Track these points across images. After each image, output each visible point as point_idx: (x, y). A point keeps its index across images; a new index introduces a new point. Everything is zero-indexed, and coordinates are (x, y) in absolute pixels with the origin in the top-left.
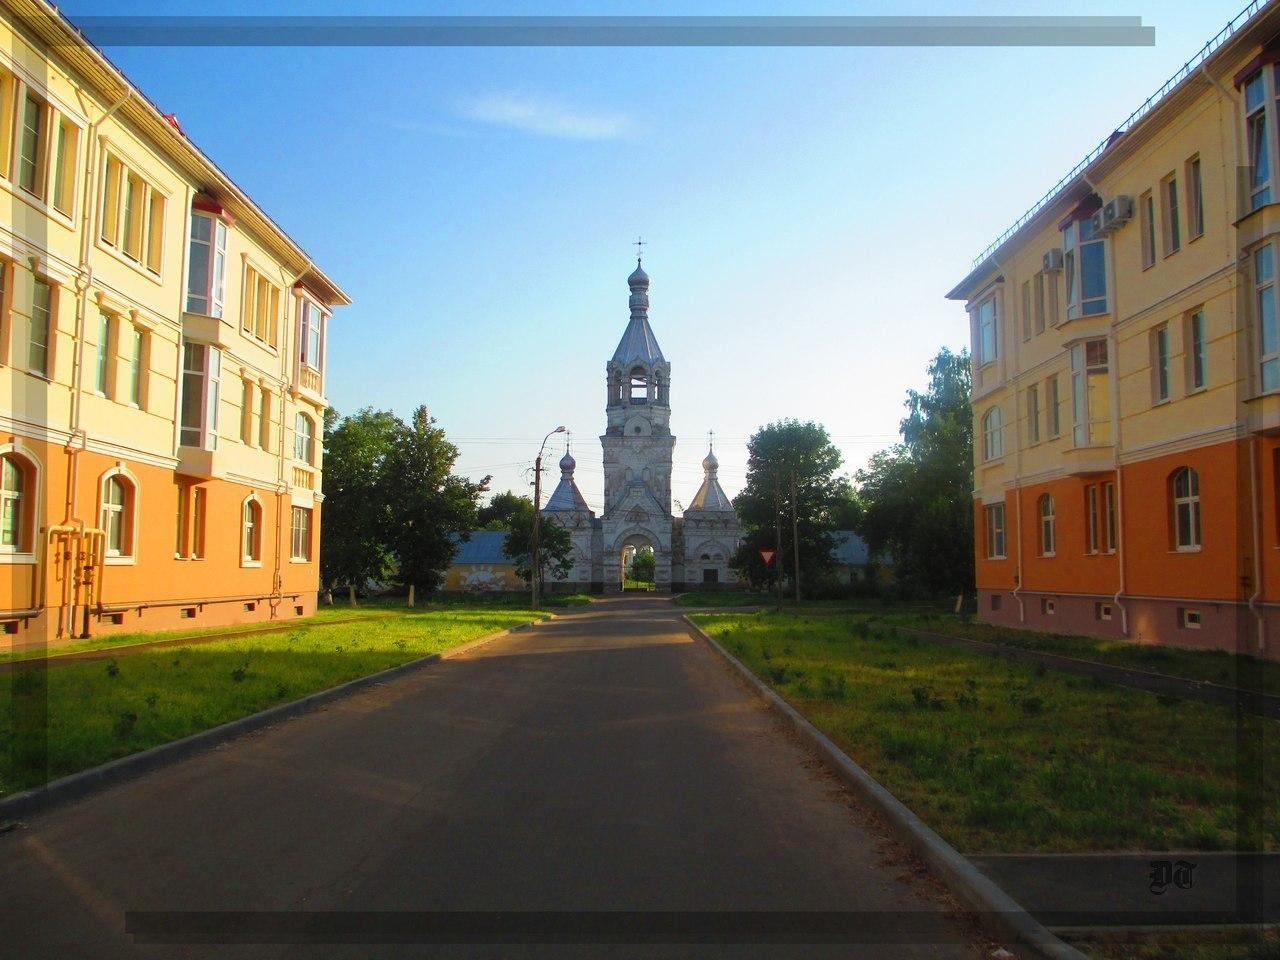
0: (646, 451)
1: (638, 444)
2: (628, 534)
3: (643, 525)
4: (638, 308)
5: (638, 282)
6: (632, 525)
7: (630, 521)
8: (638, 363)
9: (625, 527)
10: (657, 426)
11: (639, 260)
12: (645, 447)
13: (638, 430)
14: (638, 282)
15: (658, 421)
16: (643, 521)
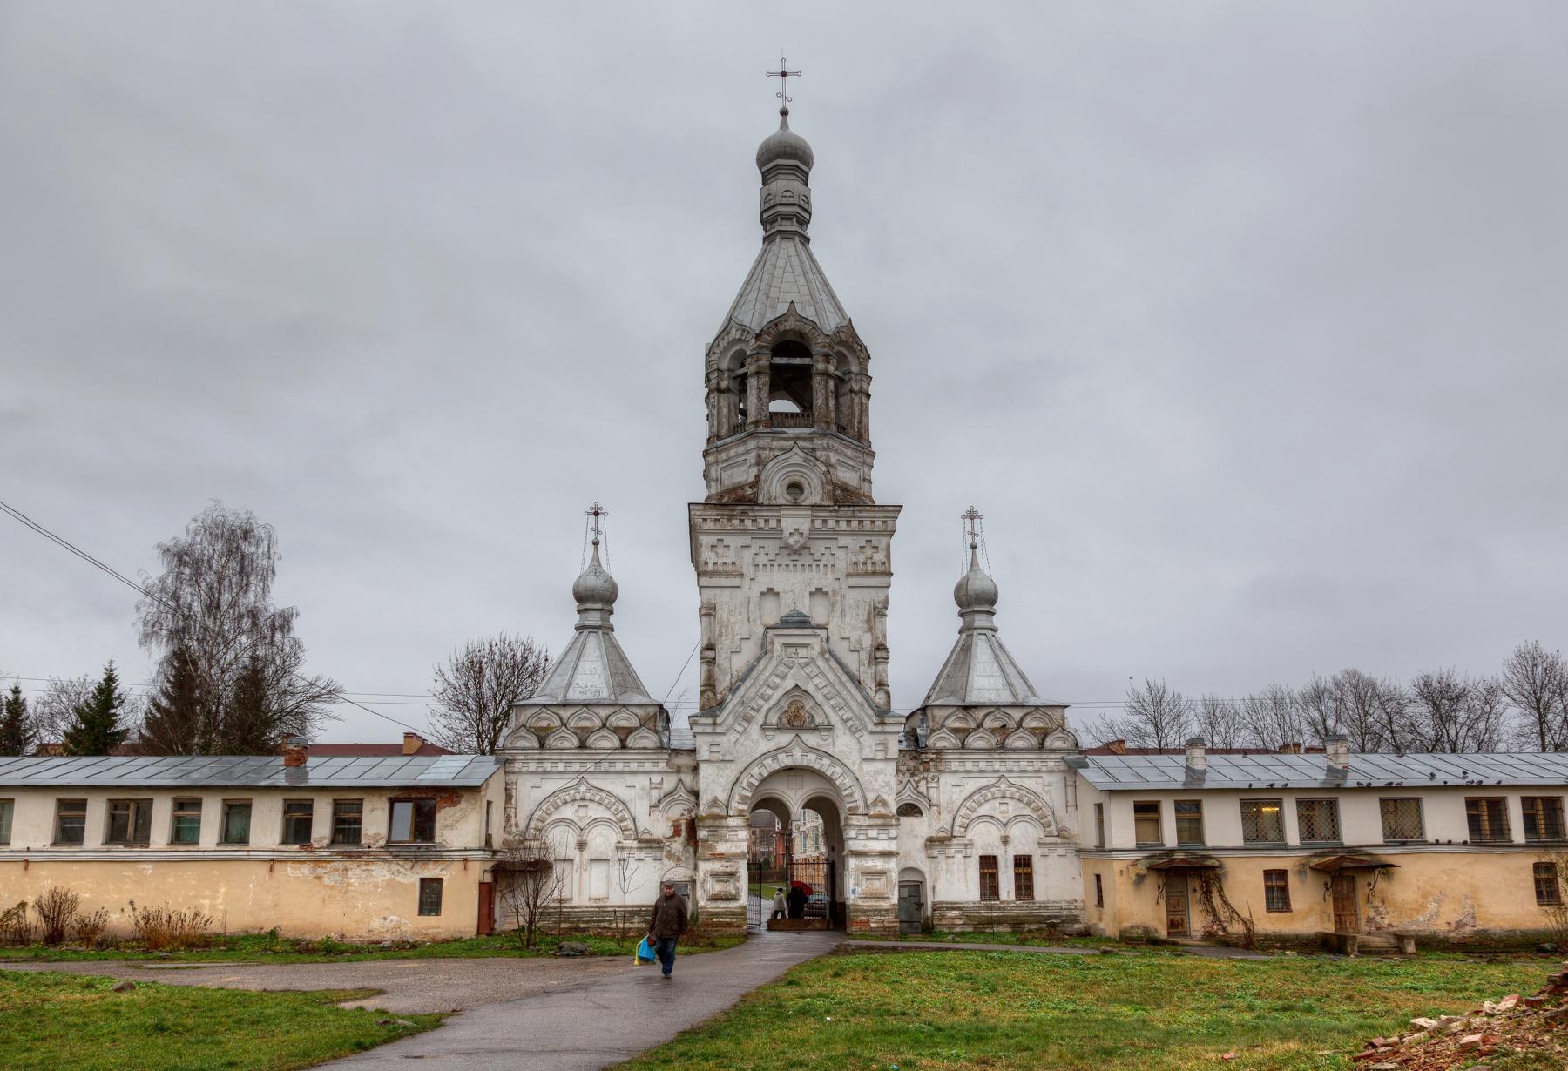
0: (818, 547)
1: (794, 524)
2: (772, 765)
3: (812, 739)
4: (785, 221)
5: (784, 161)
6: (784, 738)
7: (779, 728)
8: (789, 325)
9: (772, 745)
10: (844, 488)
11: (784, 113)
12: (814, 534)
13: (795, 487)
14: (784, 161)
15: (847, 476)
16: (816, 729)
